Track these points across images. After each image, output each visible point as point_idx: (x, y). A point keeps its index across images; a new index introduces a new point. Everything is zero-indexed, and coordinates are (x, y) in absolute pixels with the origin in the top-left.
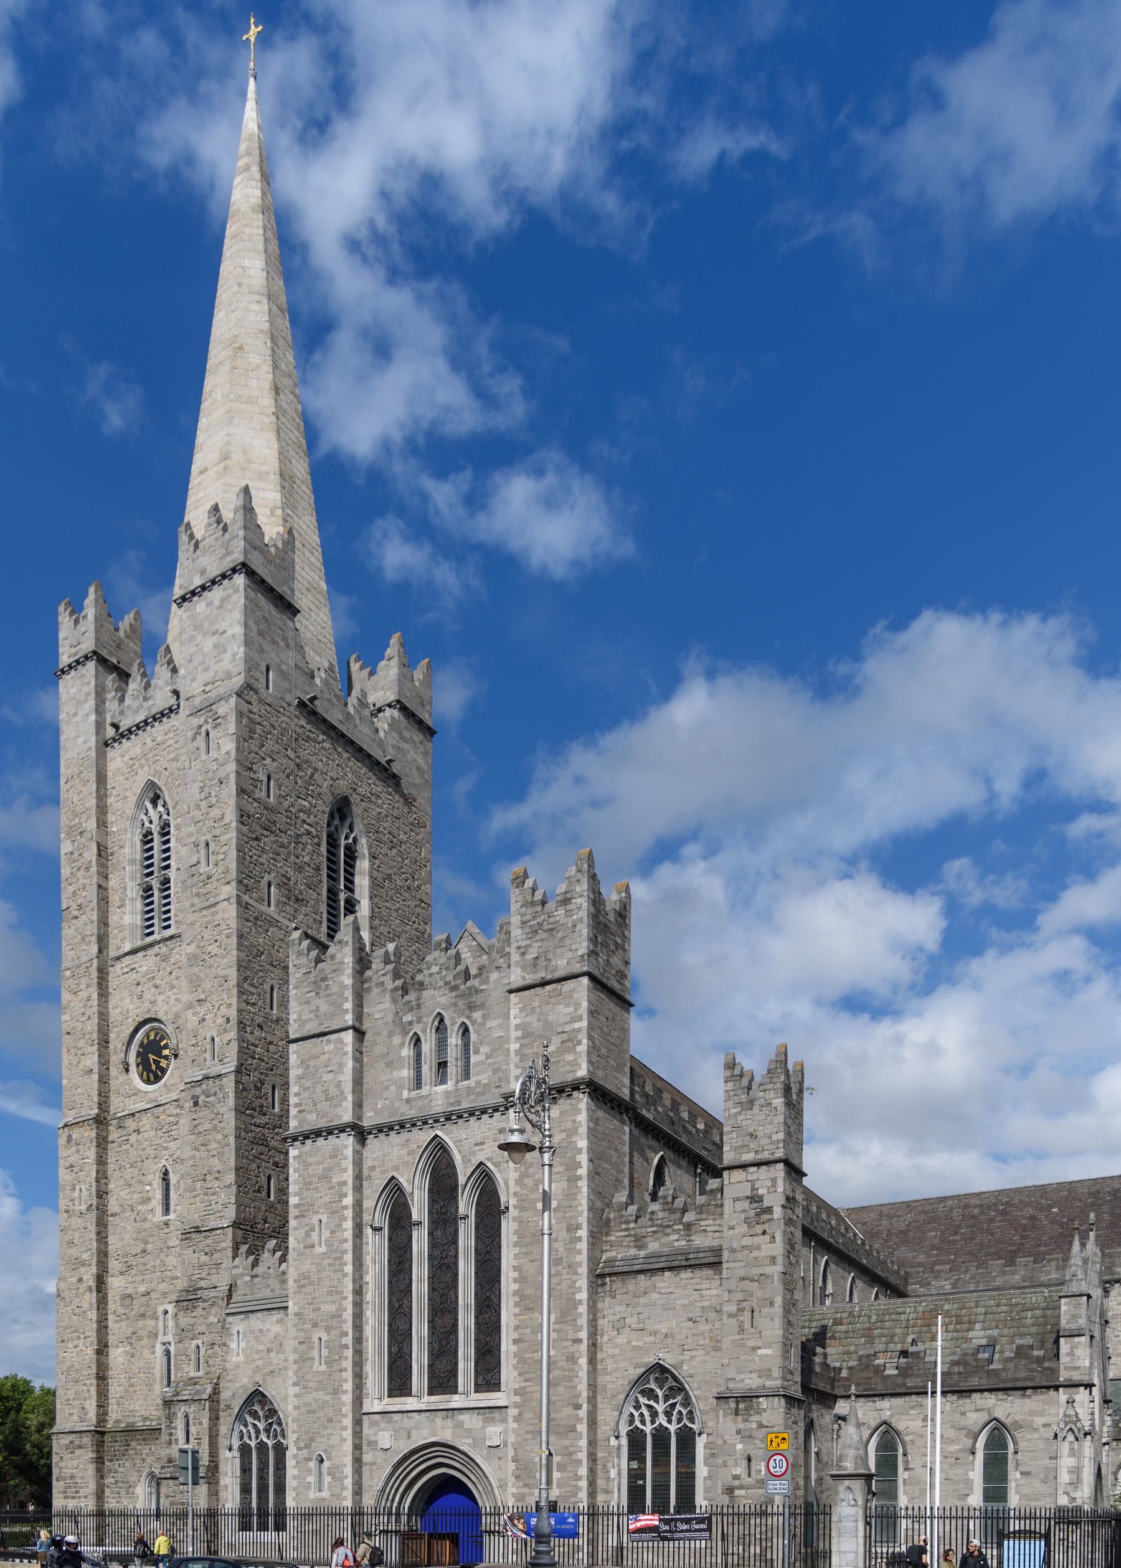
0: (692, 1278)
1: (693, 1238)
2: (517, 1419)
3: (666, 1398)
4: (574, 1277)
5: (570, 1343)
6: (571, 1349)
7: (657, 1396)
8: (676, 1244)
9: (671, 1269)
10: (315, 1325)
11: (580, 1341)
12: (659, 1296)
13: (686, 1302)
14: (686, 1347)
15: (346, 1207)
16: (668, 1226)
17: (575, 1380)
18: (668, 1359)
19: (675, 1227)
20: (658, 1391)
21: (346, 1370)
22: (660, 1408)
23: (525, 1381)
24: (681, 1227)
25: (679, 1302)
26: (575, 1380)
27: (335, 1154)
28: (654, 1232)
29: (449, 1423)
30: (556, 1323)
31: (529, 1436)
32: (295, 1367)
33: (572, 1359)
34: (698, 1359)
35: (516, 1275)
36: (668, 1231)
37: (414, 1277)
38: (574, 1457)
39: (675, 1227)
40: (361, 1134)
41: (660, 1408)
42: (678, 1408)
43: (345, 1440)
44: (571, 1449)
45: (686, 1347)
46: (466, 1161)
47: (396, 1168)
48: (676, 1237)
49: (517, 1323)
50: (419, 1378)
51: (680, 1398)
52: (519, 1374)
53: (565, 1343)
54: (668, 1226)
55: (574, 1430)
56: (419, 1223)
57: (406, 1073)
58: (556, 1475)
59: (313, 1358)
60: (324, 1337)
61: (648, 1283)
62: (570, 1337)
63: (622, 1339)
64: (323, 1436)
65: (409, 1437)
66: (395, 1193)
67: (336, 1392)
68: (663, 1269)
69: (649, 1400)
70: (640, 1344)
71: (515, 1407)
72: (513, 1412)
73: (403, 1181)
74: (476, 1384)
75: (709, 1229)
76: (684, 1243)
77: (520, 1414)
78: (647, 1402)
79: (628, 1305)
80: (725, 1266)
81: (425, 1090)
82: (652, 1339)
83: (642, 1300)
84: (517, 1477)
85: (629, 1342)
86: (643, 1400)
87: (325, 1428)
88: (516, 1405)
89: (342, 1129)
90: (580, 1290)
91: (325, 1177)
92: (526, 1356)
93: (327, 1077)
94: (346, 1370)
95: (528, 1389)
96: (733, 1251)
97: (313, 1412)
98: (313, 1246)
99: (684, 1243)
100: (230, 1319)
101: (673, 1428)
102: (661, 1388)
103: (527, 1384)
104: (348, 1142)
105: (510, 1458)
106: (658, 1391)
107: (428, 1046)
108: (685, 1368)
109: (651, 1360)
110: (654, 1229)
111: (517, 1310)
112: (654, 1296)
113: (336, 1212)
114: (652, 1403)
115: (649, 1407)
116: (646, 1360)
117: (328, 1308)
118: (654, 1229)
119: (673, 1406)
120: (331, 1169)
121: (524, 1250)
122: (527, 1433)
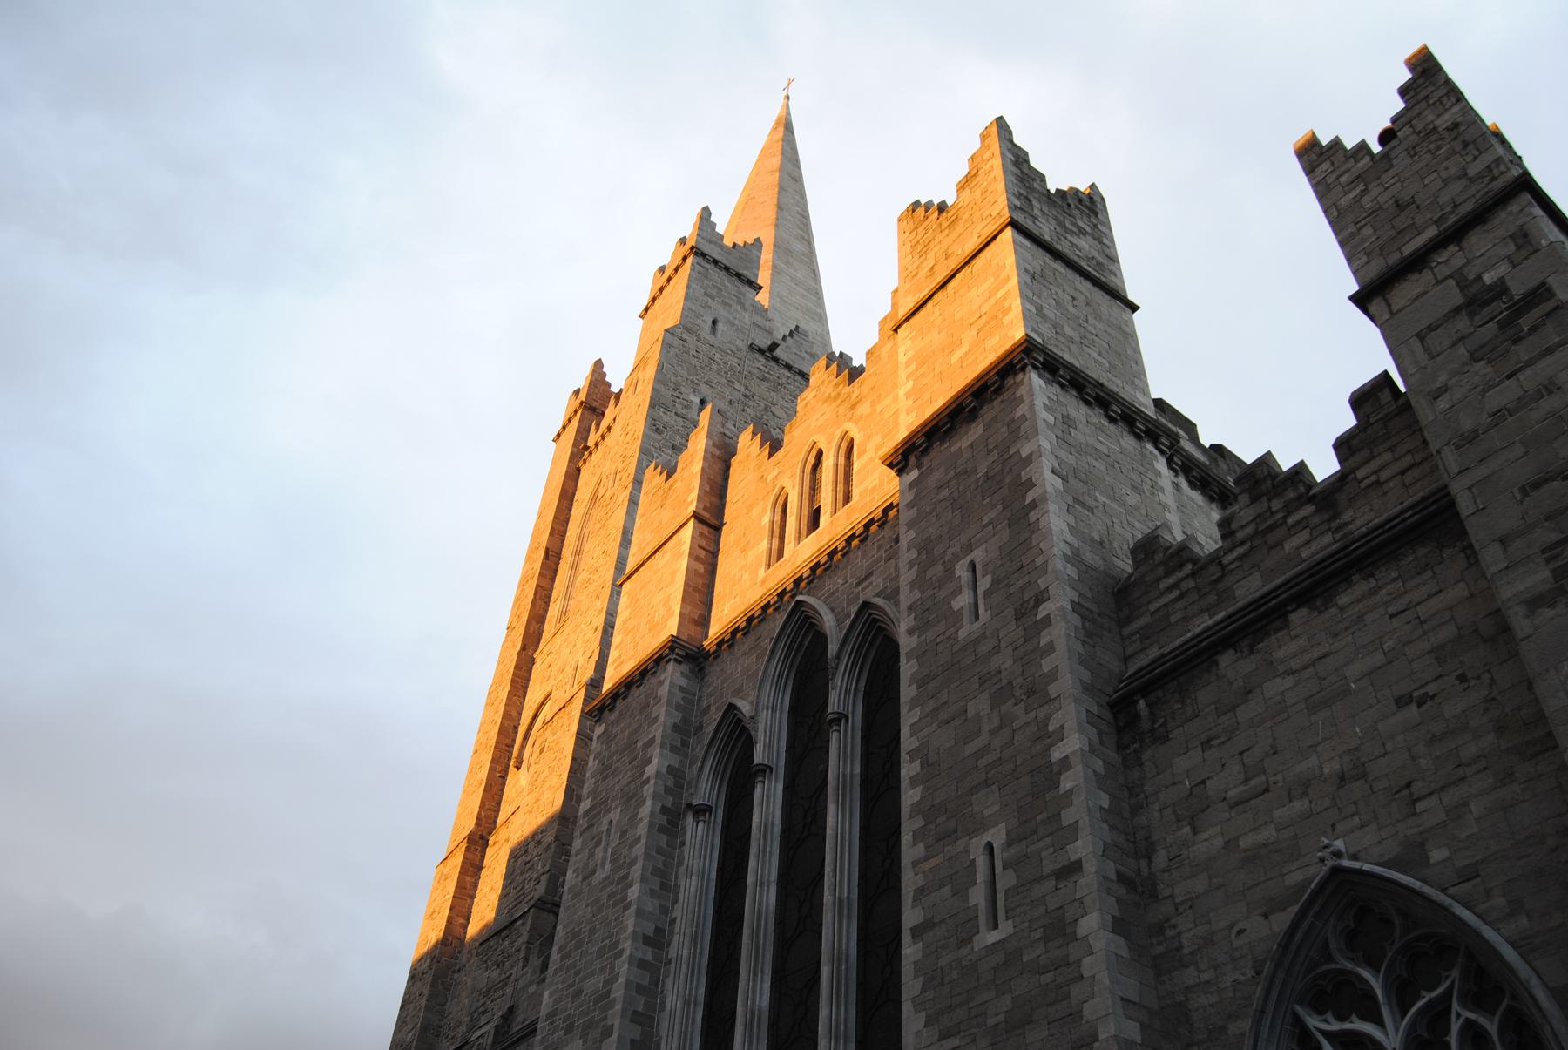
0: (1374, 592)
1: (1346, 517)
3: (1403, 996)
4: (1042, 713)
5: (1052, 883)
6: (1053, 903)
7: (1370, 996)
8: (1305, 554)
11: (1075, 867)
12: (1288, 682)
13: (1379, 658)
14: (1418, 788)
16: (1271, 528)
17: (1076, 991)
19: (1290, 521)
20: (1366, 974)
24: (1308, 510)
25: (1353, 670)
28: (1240, 558)
30: (1009, 844)
33: (1060, 929)
34: (1476, 808)
39: (1290, 521)
42: (1460, 1015)
45: (1418, 788)
49: (921, 882)
51: (1455, 973)
53: (1037, 891)
54: (1271, 528)
56: (765, 770)
61: (1248, 665)
62: (1048, 868)
63: (1209, 842)
66: (736, 732)
69: (1342, 1018)
70: (1268, 833)
73: (745, 707)
75: (1384, 475)
76: (1328, 538)
78: (1335, 1026)
79: (1206, 745)
82: (1299, 805)
85: (1230, 845)
90: (1060, 735)
99: (1328, 538)
102: (1374, 966)
106: (1366, 974)
108: (1437, 855)
109: (1307, 872)
110: (1241, 550)
112: (1275, 687)
116: (1297, 877)
118: (1241, 550)
119: (1438, 1015)
121: (931, 705)
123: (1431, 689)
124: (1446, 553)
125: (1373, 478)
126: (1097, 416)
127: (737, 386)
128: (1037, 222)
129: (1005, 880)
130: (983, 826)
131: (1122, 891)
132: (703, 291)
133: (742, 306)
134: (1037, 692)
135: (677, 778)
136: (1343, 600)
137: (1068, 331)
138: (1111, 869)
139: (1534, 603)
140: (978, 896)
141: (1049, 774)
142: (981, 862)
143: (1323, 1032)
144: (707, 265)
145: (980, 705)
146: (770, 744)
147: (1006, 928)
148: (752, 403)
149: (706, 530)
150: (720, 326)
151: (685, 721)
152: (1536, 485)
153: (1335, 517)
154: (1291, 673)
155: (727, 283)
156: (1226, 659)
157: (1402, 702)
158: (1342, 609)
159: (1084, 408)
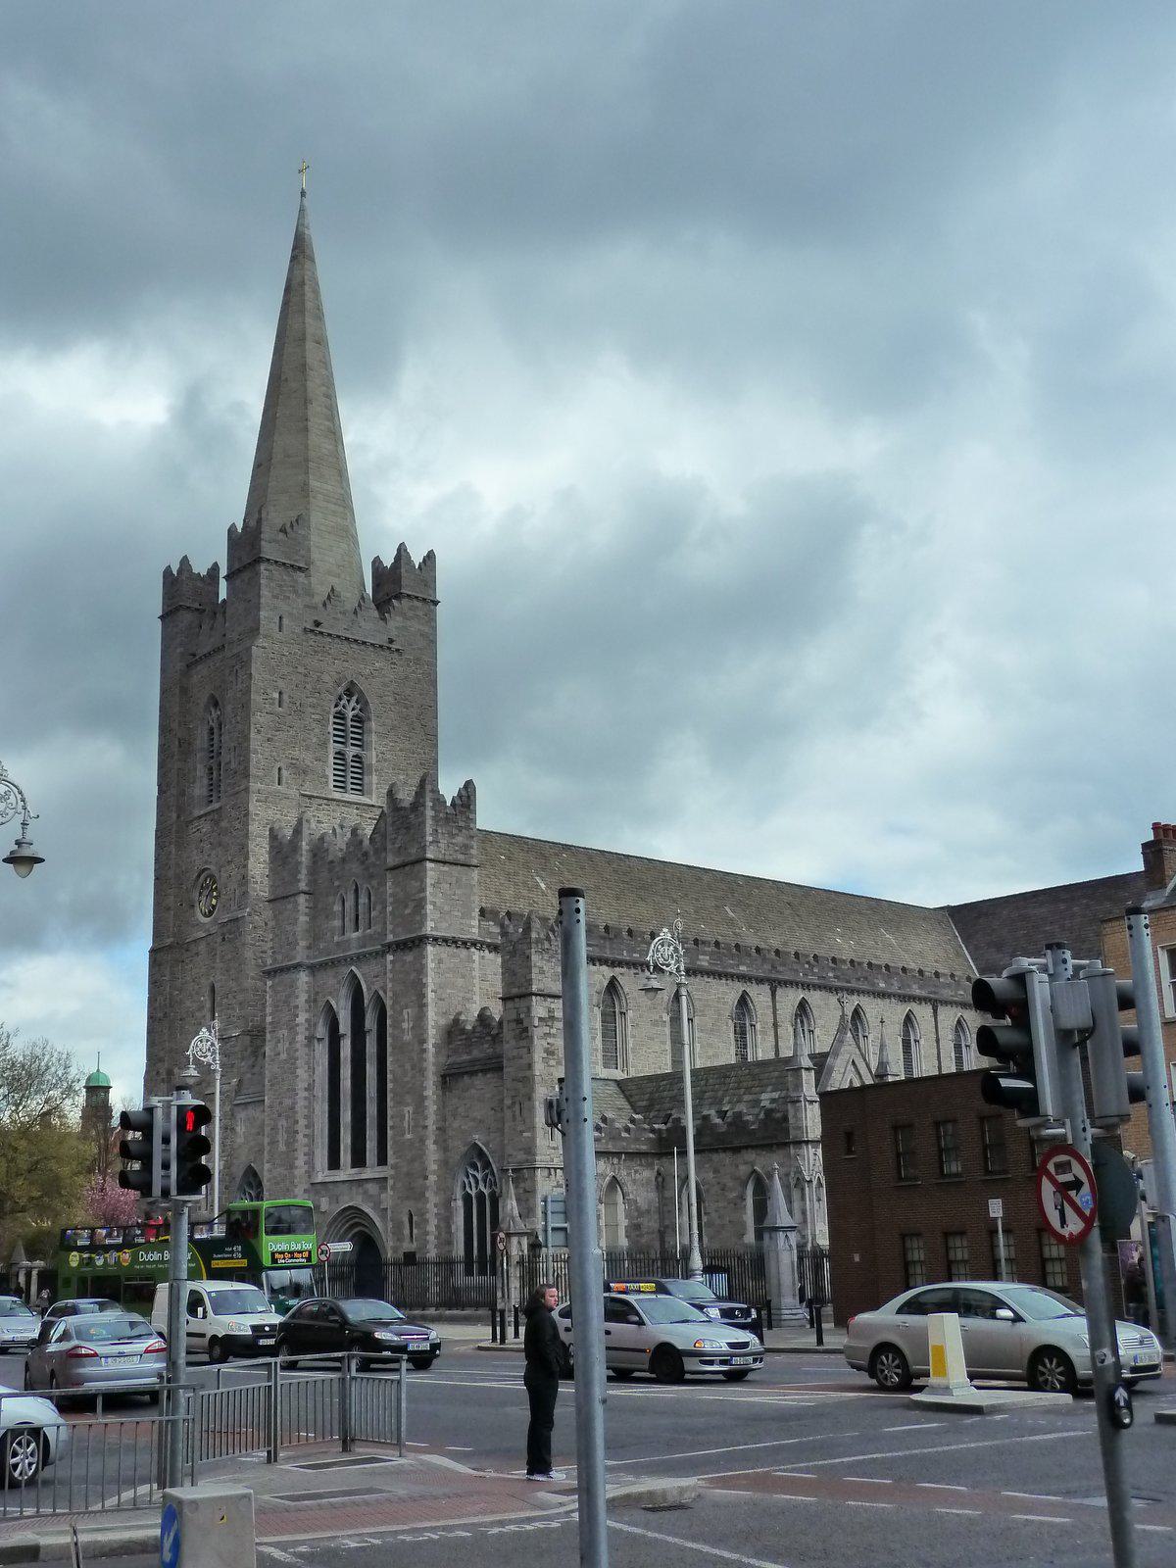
2: (392, 1188)
9: (482, 1071)
15: (297, 1025)
18: (478, 1138)
22: (479, 1176)
27: (292, 985)
30: (414, 1113)
32: (269, 1148)
33: (422, 1141)
37: (342, 1077)
40: (313, 969)
41: (479, 1176)
42: (489, 1177)
46: (369, 989)
47: (330, 994)
48: (486, 1046)
50: (345, 1156)
55: (423, 1195)
57: (337, 923)
58: (415, 1231)
63: (456, 1125)
67: (292, 1167)
72: (390, 1182)
73: (333, 1003)
80: (505, 1070)
81: (347, 934)
83: (467, 1094)
84: (393, 1233)
85: (460, 1126)
86: (471, 1171)
88: (392, 1177)
89: (297, 967)
91: (286, 1002)
93: (288, 928)
96: (509, 1060)
97: (277, 1183)
98: (279, 1054)
100: (236, 1108)
101: (486, 1192)
104: (303, 977)
107: (350, 903)
112: (473, 1091)
113: (292, 1028)
114: (475, 1173)
117: (288, 1102)
120: (289, 996)
126: (452, 950)
127: (301, 669)
128: (439, 845)
130: (408, 1105)
131: (437, 1132)
132: (270, 595)
133: (296, 592)
134: (422, 1071)
135: (311, 1024)
136: (488, 1076)
137: (446, 908)
138: (434, 1127)
139: (509, 1108)
140: (406, 1125)
141: (423, 1098)
142: (407, 1115)
144: (271, 567)
145: (408, 1066)
146: (345, 1026)
147: (408, 1136)
148: (309, 679)
149: (307, 896)
150: (285, 621)
151: (309, 997)
154: (477, 1090)
155: (285, 577)
156: (466, 1077)
157: (492, 1109)
159: (447, 948)
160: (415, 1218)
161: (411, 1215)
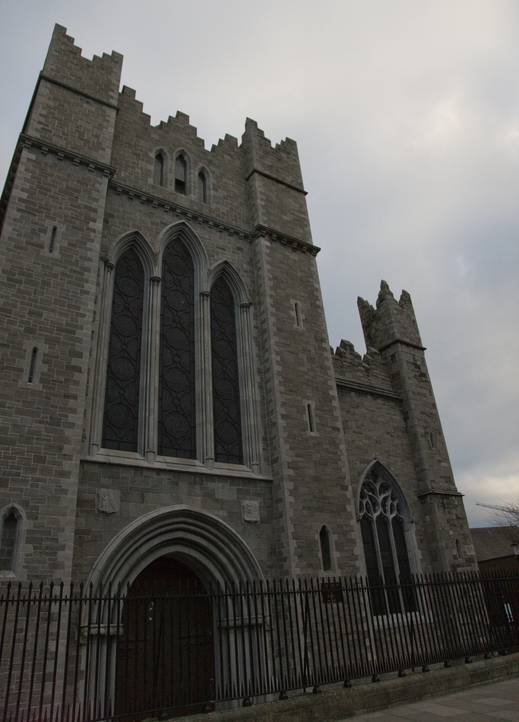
10: (30, 331)
12: (366, 411)
21: (75, 397)
23: (297, 456)
26: (339, 463)
29: (197, 489)
30: (317, 409)
31: (305, 512)
35: (278, 358)
36: (355, 368)
38: (348, 536)
43: (65, 492)
44: (345, 528)
49: (284, 401)
52: (290, 449)
55: (345, 510)
59: (22, 370)
60: (44, 348)
64: (25, 481)
65: (143, 501)
68: (365, 393)
71: (290, 480)
74: (216, 453)
76: (366, 380)
77: (296, 488)
84: (300, 556)
87: (33, 470)
92: (295, 432)
94: (75, 397)
95: (300, 464)
103: (299, 459)
105: (290, 534)
111: (282, 389)
115: (371, 498)
122: (304, 508)
123: (393, 434)
124: (397, 408)
125: (376, 375)
129: (315, 420)
143: (369, 495)
152: (423, 413)
153: (368, 376)
158: (378, 403)
160: (333, 538)
161: (324, 533)
